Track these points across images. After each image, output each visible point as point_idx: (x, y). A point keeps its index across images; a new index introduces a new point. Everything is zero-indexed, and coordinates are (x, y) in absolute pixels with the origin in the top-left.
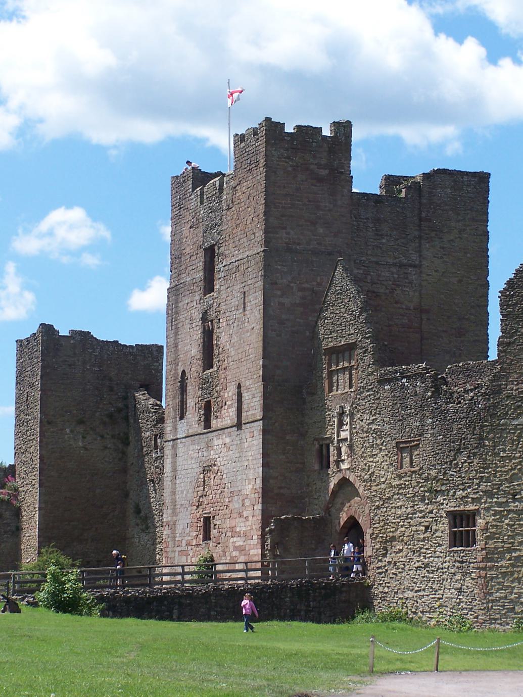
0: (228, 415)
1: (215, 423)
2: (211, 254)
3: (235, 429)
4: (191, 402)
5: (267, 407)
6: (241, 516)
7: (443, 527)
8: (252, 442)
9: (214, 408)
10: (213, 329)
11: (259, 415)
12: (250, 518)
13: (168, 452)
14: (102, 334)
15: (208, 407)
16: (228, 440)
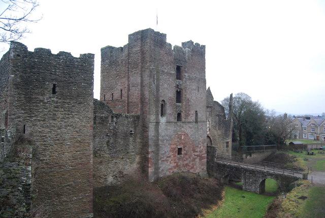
1: (183, 120)
6: (198, 146)
9: (183, 115)
10: (180, 91)
12: (202, 147)
15: (179, 115)
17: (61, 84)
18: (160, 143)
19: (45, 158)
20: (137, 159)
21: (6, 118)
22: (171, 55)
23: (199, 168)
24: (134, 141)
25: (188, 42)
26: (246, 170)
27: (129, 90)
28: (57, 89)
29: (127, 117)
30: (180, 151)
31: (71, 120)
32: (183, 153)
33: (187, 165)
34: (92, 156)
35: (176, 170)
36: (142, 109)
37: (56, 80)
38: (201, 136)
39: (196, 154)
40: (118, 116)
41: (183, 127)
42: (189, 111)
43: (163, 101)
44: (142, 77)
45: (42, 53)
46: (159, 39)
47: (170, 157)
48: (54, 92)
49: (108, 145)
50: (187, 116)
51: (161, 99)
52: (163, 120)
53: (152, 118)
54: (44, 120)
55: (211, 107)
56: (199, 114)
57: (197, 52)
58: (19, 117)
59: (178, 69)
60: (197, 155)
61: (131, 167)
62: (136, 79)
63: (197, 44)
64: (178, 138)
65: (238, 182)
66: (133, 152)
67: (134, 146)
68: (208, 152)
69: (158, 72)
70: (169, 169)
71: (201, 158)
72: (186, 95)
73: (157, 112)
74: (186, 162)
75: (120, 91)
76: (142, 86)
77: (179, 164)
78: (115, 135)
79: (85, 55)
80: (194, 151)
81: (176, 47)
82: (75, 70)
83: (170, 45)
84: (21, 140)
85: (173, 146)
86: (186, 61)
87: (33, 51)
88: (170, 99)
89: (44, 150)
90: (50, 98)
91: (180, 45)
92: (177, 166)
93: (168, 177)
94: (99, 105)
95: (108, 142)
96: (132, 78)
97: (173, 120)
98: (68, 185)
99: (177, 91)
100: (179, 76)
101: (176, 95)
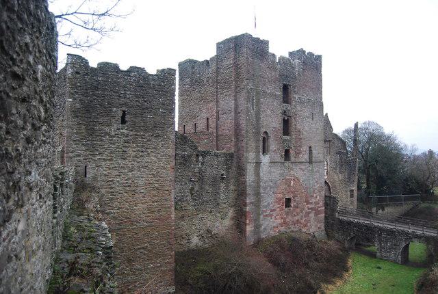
1: (293, 159)
3: (307, 164)
9: (292, 152)
10: (288, 119)
15: (287, 152)
16: (303, 167)
17: (132, 110)
18: (262, 191)
19: (112, 211)
20: (231, 213)
21: (62, 157)
22: (275, 70)
23: (314, 227)
24: (227, 186)
25: (298, 51)
26: (381, 230)
27: (218, 118)
28: (128, 118)
29: (217, 156)
30: (288, 202)
31: (146, 159)
32: (292, 205)
33: (298, 222)
34: (173, 208)
35: (283, 229)
36: (236, 145)
37: (125, 105)
38: (317, 182)
39: (310, 206)
40: (204, 154)
41: (292, 169)
42: (300, 146)
43: (266, 133)
44: (236, 100)
45: (108, 69)
46: (259, 48)
48: (123, 122)
49: (192, 194)
50: (298, 153)
51: (263, 130)
53: (251, 156)
54: (111, 160)
55: (330, 141)
57: (311, 64)
58: (79, 156)
59: (285, 88)
60: (311, 209)
61: (222, 224)
62: (228, 103)
63: (311, 54)
64: (286, 184)
65: (369, 246)
66: (225, 203)
67: (226, 194)
68: (326, 204)
69: (258, 93)
70: (274, 227)
71: (317, 212)
72: (297, 124)
73: (257, 148)
74: (296, 218)
75: (205, 120)
76: (237, 113)
77: (287, 220)
78: (201, 179)
79: (163, 70)
80: (308, 203)
81: (282, 58)
82: (150, 91)
83: (274, 55)
84: (81, 186)
85: (279, 196)
86: (295, 78)
87: (95, 66)
88: (275, 130)
89: (111, 199)
90: (119, 129)
91: (287, 56)
92: (285, 223)
93: (273, 238)
94: (182, 139)
95: (192, 189)
96: (222, 103)
97: (278, 160)
98: (143, 248)
99: (284, 119)
100: (286, 98)
101: (282, 125)
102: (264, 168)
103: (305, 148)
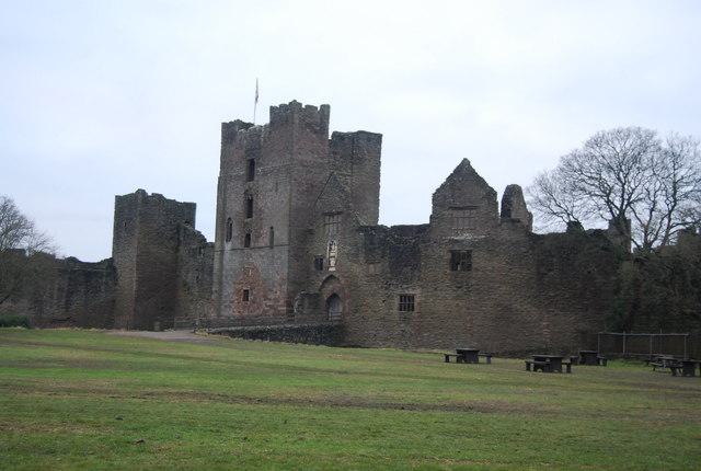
0: (264, 241)
1: (252, 244)
2: (252, 165)
3: (267, 250)
4: (234, 234)
5: (290, 239)
7: (397, 301)
8: (283, 255)
11: (285, 241)
13: (217, 257)
14: (168, 196)
15: (248, 236)
47: (232, 302)
52: (228, 246)
56: (276, 233)
72: (259, 203)
80: (266, 298)
97: (239, 246)
100: (251, 175)
102: (227, 256)
103: (266, 230)
